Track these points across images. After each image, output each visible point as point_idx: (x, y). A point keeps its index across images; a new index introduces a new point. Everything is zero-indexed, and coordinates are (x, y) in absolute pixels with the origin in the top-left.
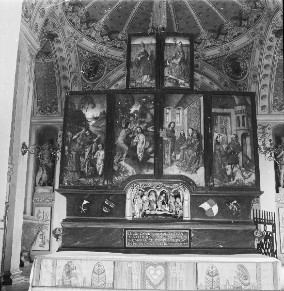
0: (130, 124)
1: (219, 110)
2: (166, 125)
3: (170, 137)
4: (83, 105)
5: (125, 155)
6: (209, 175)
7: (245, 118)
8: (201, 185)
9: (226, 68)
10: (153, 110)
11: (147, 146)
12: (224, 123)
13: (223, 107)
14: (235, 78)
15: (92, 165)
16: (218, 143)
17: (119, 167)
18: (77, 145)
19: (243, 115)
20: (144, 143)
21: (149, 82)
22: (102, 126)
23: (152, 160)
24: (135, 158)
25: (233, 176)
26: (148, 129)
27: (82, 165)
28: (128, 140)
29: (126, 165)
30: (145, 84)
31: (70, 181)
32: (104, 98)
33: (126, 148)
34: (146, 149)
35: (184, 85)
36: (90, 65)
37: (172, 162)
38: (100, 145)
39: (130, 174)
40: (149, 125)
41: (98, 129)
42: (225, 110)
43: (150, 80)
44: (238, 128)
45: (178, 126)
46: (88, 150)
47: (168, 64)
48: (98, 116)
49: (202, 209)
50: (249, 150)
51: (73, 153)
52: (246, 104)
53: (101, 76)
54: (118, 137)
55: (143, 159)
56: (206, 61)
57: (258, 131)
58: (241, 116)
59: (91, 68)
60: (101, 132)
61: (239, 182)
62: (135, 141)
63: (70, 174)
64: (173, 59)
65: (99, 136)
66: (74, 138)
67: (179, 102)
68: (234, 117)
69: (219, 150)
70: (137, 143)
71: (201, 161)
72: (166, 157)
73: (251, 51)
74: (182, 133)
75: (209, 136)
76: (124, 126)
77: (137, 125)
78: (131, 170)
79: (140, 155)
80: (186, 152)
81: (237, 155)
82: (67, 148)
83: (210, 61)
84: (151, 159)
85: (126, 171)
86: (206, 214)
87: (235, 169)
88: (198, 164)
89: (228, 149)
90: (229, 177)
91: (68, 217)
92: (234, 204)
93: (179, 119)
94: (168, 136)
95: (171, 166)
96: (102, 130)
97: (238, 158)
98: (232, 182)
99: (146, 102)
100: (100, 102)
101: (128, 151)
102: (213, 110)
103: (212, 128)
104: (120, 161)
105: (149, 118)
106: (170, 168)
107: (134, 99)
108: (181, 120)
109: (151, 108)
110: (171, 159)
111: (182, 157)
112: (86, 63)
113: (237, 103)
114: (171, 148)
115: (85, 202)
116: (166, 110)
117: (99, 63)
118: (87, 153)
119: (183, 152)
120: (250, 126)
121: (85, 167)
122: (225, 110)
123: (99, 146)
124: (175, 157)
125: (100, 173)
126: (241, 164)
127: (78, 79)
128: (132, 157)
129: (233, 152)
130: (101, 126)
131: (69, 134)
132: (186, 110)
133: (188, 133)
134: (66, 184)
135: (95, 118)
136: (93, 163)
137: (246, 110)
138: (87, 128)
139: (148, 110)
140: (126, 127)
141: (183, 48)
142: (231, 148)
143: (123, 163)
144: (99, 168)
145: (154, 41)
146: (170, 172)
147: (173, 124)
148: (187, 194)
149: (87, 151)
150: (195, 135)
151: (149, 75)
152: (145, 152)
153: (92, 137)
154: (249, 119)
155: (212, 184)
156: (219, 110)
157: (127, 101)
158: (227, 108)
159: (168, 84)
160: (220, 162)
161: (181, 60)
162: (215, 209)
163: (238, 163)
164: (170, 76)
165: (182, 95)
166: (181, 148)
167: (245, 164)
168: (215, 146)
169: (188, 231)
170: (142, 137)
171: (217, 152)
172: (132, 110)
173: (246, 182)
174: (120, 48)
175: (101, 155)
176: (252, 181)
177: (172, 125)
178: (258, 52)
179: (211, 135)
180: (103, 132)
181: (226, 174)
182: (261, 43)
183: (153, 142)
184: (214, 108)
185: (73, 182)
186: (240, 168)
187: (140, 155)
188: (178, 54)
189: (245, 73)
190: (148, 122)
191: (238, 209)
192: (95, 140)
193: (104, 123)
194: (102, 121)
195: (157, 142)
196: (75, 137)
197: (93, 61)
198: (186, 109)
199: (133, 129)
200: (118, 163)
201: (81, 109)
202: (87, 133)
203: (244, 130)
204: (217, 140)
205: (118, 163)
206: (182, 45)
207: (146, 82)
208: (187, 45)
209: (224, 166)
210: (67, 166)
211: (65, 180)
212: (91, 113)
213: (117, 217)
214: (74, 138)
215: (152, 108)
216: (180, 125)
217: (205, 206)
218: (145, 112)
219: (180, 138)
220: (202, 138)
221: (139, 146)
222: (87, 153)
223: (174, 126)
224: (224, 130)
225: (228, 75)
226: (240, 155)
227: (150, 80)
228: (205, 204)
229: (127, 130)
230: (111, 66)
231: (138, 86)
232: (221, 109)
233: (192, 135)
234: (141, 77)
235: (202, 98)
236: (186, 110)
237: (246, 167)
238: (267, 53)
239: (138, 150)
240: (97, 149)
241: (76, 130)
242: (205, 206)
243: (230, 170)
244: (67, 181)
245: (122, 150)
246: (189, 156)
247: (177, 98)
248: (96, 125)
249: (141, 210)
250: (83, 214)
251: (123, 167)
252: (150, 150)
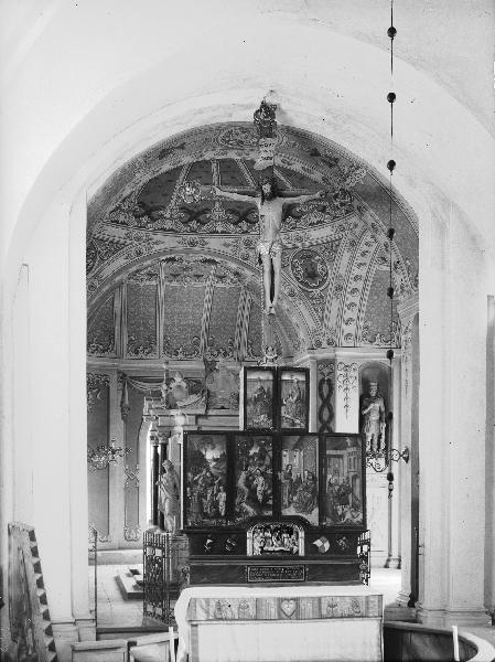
2: (284, 468)
6: (322, 517)
9: (294, 267)
13: (336, 449)
16: (330, 484)
23: (271, 502)
25: (343, 515)
33: (247, 490)
37: (290, 503)
42: (339, 452)
57: (339, 373)
58: (352, 458)
73: (336, 251)
75: (323, 478)
78: (251, 511)
79: (260, 497)
85: (247, 513)
93: (296, 461)
99: (265, 444)
100: (220, 443)
103: (326, 470)
115: (209, 541)
122: (339, 452)
128: (252, 499)
129: (344, 494)
131: (189, 475)
135: (215, 460)
136: (215, 504)
138: (208, 470)
140: (246, 469)
145: (271, 377)
159: (285, 425)
162: (327, 546)
170: (261, 479)
172: (252, 452)
174: (123, 223)
175: (223, 495)
178: (346, 256)
182: (353, 244)
187: (260, 497)
189: (324, 281)
193: (224, 465)
195: (275, 484)
212: (211, 455)
217: (318, 543)
221: (259, 488)
224: (336, 472)
226: (350, 496)
231: (256, 426)
235: (317, 440)
237: (355, 508)
238: (361, 260)
240: (219, 491)
242: (318, 543)
245: (243, 492)
247: (294, 440)
250: (208, 553)
252: (269, 492)
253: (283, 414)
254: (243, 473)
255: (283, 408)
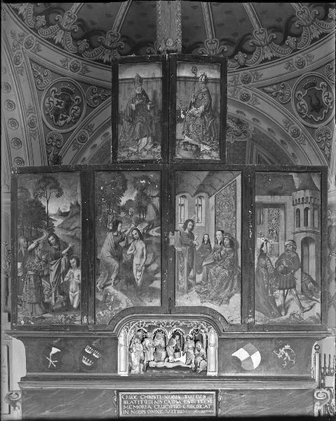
0: (120, 225)
1: (267, 199)
2: (180, 226)
3: (185, 245)
4: (41, 191)
5: (113, 277)
6: (248, 306)
7: (309, 212)
8: (234, 323)
9: (297, 101)
10: (158, 198)
11: (149, 261)
12: (274, 221)
13: (273, 193)
14: (311, 121)
15: (62, 293)
16: (262, 254)
17: (106, 296)
18: (36, 260)
19: (306, 206)
20: (145, 257)
21: (150, 150)
22: (75, 228)
23: (157, 284)
24: (131, 281)
25: (285, 307)
26: (151, 233)
27: (47, 293)
28: (118, 252)
29: (116, 292)
30: (144, 153)
31: (29, 319)
32: (76, 178)
33: (115, 264)
34: (147, 266)
35: (209, 154)
36: (56, 96)
37: (190, 286)
38: (73, 260)
39: (124, 306)
40: (151, 225)
41: (70, 233)
43: (153, 147)
44: (297, 230)
45: (199, 228)
46: (54, 268)
47: (183, 116)
48: (68, 210)
49: (238, 360)
50: (312, 266)
51: (30, 272)
52: (313, 188)
53: (77, 118)
54: (101, 246)
55: (143, 282)
56: (262, 88)
58: (302, 208)
59: (59, 103)
60: (73, 237)
61: (294, 317)
62: (129, 252)
63: (28, 306)
64: (190, 108)
65: (70, 245)
66: (30, 248)
67: (201, 185)
68: (291, 210)
69: (266, 267)
70: (133, 256)
71: (236, 284)
72: (180, 279)
74: (206, 239)
75: (248, 244)
76: (111, 228)
77: (133, 226)
78: (125, 302)
80: (212, 270)
81: (293, 274)
82: (19, 265)
83: (269, 89)
84: (155, 282)
85: (117, 302)
86: (242, 366)
87: (289, 297)
88: (231, 290)
89: (279, 265)
90: (279, 309)
91: (29, 374)
92: (285, 350)
93: (201, 214)
94: (182, 244)
95: (188, 292)
96: (75, 235)
97: (294, 279)
98: (284, 318)
100: (70, 186)
101: (119, 269)
102: (257, 199)
103: (254, 230)
104: (105, 286)
105: (151, 214)
106: (186, 296)
107: (126, 181)
108: (204, 216)
109: (155, 197)
110: (188, 281)
111: (206, 278)
112: (48, 95)
113: (297, 187)
114: (188, 264)
115: (54, 350)
116: (179, 200)
117: (72, 93)
118: (53, 274)
119: (207, 269)
120: (316, 225)
121: (51, 295)
122: (277, 199)
123: (71, 261)
124: (194, 278)
125: (75, 306)
126: (298, 288)
127: (38, 125)
129: (286, 271)
130: (73, 227)
131: (22, 240)
132: (212, 200)
133: (216, 239)
134: (23, 322)
136: (63, 290)
137: (311, 197)
138: (51, 232)
139: (149, 199)
140: (115, 229)
141: (209, 85)
142: (284, 263)
143: (111, 289)
144: (74, 298)
146: (186, 303)
147: (190, 223)
148: (213, 336)
149: (52, 270)
150: (227, 242)
151: (150, 138)
152: (146, 271)
153: (59, 247)
154: (316, 213)
155: (252, 320)
156: (267, 199)
157: (114, 185)
158: (280, 195)
160: (266, 285)
161: (205, 108)
162: (257, 358)
163: (294, 287)
164: (187, 139)
165: (206, 173)
166: (204, 264)
167: (305, 288)
168: (259, 259)
169: (214, 393)
170: (140, 245)
171: (262, 270)
172: (124, 200)
173: (306, 316)
176: (316, 315)
177: (189, 226)
179: (253, 241)
180: (78, 239)
181: (275, 304)
183: (158, 254)
184: (258, 195)
185: (34, 319)
186: (297, 295)
187: (138, 276)
188: (200, 96)
190: (150, 220)
191: (292, 358)
192: (64, 252)
193: (78, 222)
194: (74, 218)
195: (165, 250)
196: (32, 246)
197: (63, 90)
198: (213, 197)
199: (126, 233)
200: (103, 288)
201: (39, 199)
202: (50, 239)
203: (306, 232)
204: (261, 251)
205: (103, 288)
206: (207, 81)
207: (145, 150)
208: (215, 79)
209: (272, 292)
210: (21, 294)
211: (20, 315)
212: (54, 207)
213: (105, 372)
214: (30, 248)
215: (157, 196)
216: (203, 225)
217: (241, 354)
218: (144, 203)
219: (202, 247)
220: (237, 248)
221: (136, 261)
222: (53, 274)
223: (193, 226)
224: (273, 233)
225: (301, 114)
226: (298, 274)
227: (153, 147)
228: (241, 350)
229: (115, 234)
230: (95, 99)
231: (133, 158)
232: (269, 197)
233: (222, 243)
234: (138, 140)
235: (239, 178)
236: (212, 200)
237: (307, 294)
239: (134, 267)
240: (69, 266)
241: (33, 234)
242: (241, 354)
243: (281, 298)
244: (25, 319)
246: (217, 277)
247: (197, 178)
248: (66, 226)
249: (141, 361)
250: (52, 369)
251: (111, 296)
252: (154, 267)
253: (179, 136)
254: (110, 236)
255: (180, 127)
